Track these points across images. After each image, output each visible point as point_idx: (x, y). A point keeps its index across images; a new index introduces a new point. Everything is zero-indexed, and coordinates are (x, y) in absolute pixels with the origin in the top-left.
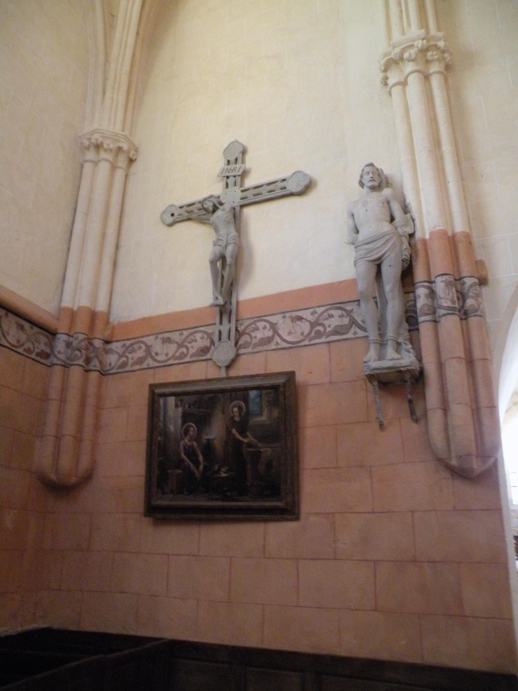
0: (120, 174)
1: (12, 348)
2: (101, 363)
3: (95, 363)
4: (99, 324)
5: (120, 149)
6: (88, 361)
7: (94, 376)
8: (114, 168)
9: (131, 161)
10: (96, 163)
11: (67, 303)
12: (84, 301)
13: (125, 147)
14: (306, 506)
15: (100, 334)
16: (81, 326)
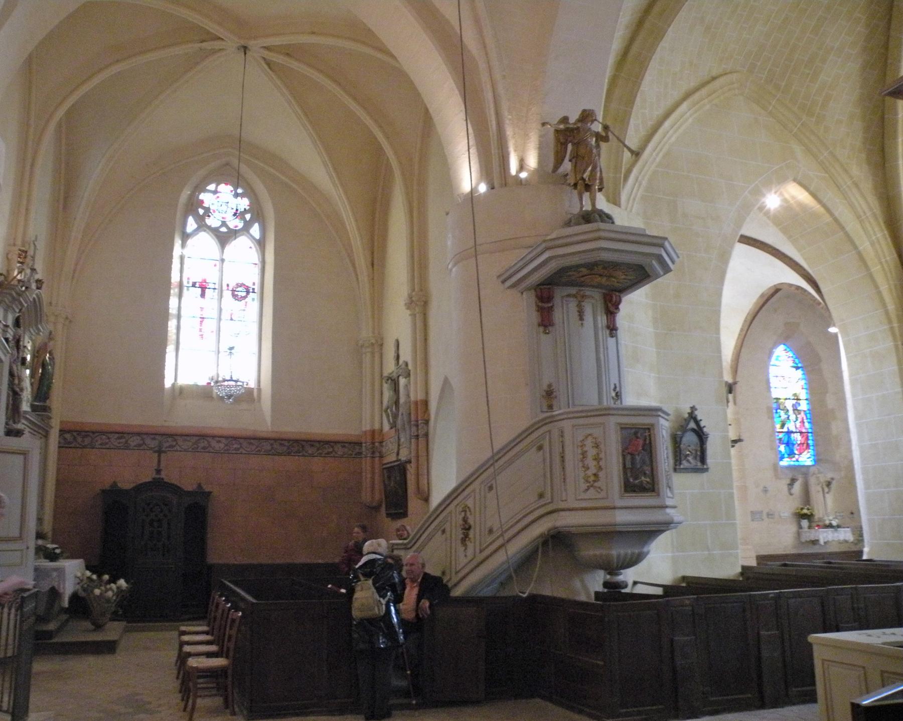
0: (377, 356)
1: (342, 457)
2: (380, 452)
3: (377, 454)
4: (377, 436)
5: (373, 344)
6: (373, 453)
7: (377, 459)
8: (373, 354)
9: (382, 345)
10: (365, 353)
11: (364, 429)
12: (368, 428)
13: (373, 341)
14: (410, 511)
15: (377, 439)
16: (369, 439)
